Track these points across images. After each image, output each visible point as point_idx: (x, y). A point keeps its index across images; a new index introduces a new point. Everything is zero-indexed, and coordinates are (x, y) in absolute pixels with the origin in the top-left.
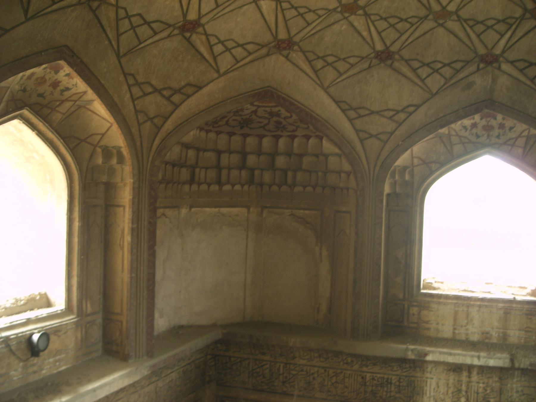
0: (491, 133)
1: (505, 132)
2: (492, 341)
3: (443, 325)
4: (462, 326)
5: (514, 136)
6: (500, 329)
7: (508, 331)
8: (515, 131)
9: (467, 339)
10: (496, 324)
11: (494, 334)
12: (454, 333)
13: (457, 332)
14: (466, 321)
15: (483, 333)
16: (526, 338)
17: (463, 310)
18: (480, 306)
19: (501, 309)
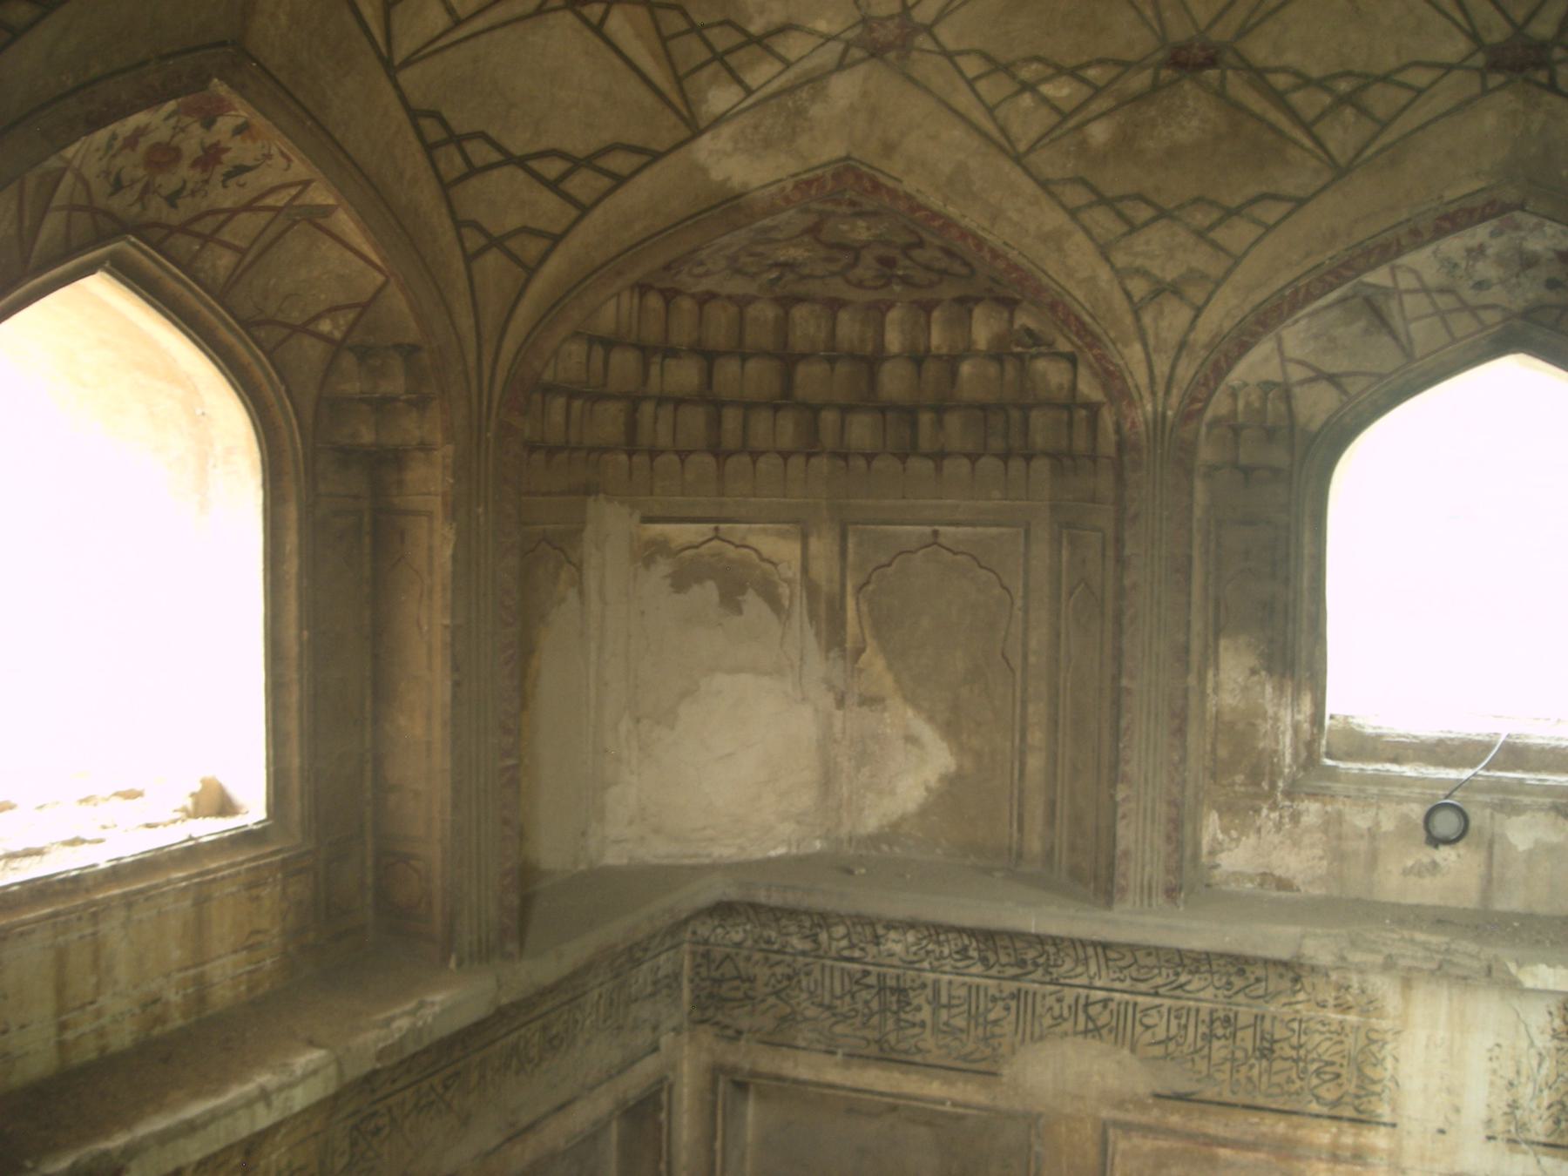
0: (159, 179)
1: (206, 182)
2: (170, 1027)
3: (23, 1027)
4: (82, 1007)
5: (228, 204)
6: (186, 969)
7: (207, 967)
8: (242, 186)
9: (103, 1049)
10: (176, 954)
11: (173, 997)
12: (62, 1046)
13: (69, 1035)
14: (93, 980)
15: (144, 1006)
16: (250, 972)
17: (81, 937)
18: (128, 901)
19: (185, 888)
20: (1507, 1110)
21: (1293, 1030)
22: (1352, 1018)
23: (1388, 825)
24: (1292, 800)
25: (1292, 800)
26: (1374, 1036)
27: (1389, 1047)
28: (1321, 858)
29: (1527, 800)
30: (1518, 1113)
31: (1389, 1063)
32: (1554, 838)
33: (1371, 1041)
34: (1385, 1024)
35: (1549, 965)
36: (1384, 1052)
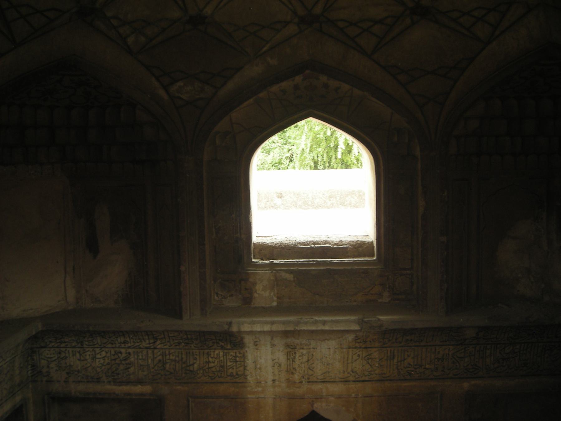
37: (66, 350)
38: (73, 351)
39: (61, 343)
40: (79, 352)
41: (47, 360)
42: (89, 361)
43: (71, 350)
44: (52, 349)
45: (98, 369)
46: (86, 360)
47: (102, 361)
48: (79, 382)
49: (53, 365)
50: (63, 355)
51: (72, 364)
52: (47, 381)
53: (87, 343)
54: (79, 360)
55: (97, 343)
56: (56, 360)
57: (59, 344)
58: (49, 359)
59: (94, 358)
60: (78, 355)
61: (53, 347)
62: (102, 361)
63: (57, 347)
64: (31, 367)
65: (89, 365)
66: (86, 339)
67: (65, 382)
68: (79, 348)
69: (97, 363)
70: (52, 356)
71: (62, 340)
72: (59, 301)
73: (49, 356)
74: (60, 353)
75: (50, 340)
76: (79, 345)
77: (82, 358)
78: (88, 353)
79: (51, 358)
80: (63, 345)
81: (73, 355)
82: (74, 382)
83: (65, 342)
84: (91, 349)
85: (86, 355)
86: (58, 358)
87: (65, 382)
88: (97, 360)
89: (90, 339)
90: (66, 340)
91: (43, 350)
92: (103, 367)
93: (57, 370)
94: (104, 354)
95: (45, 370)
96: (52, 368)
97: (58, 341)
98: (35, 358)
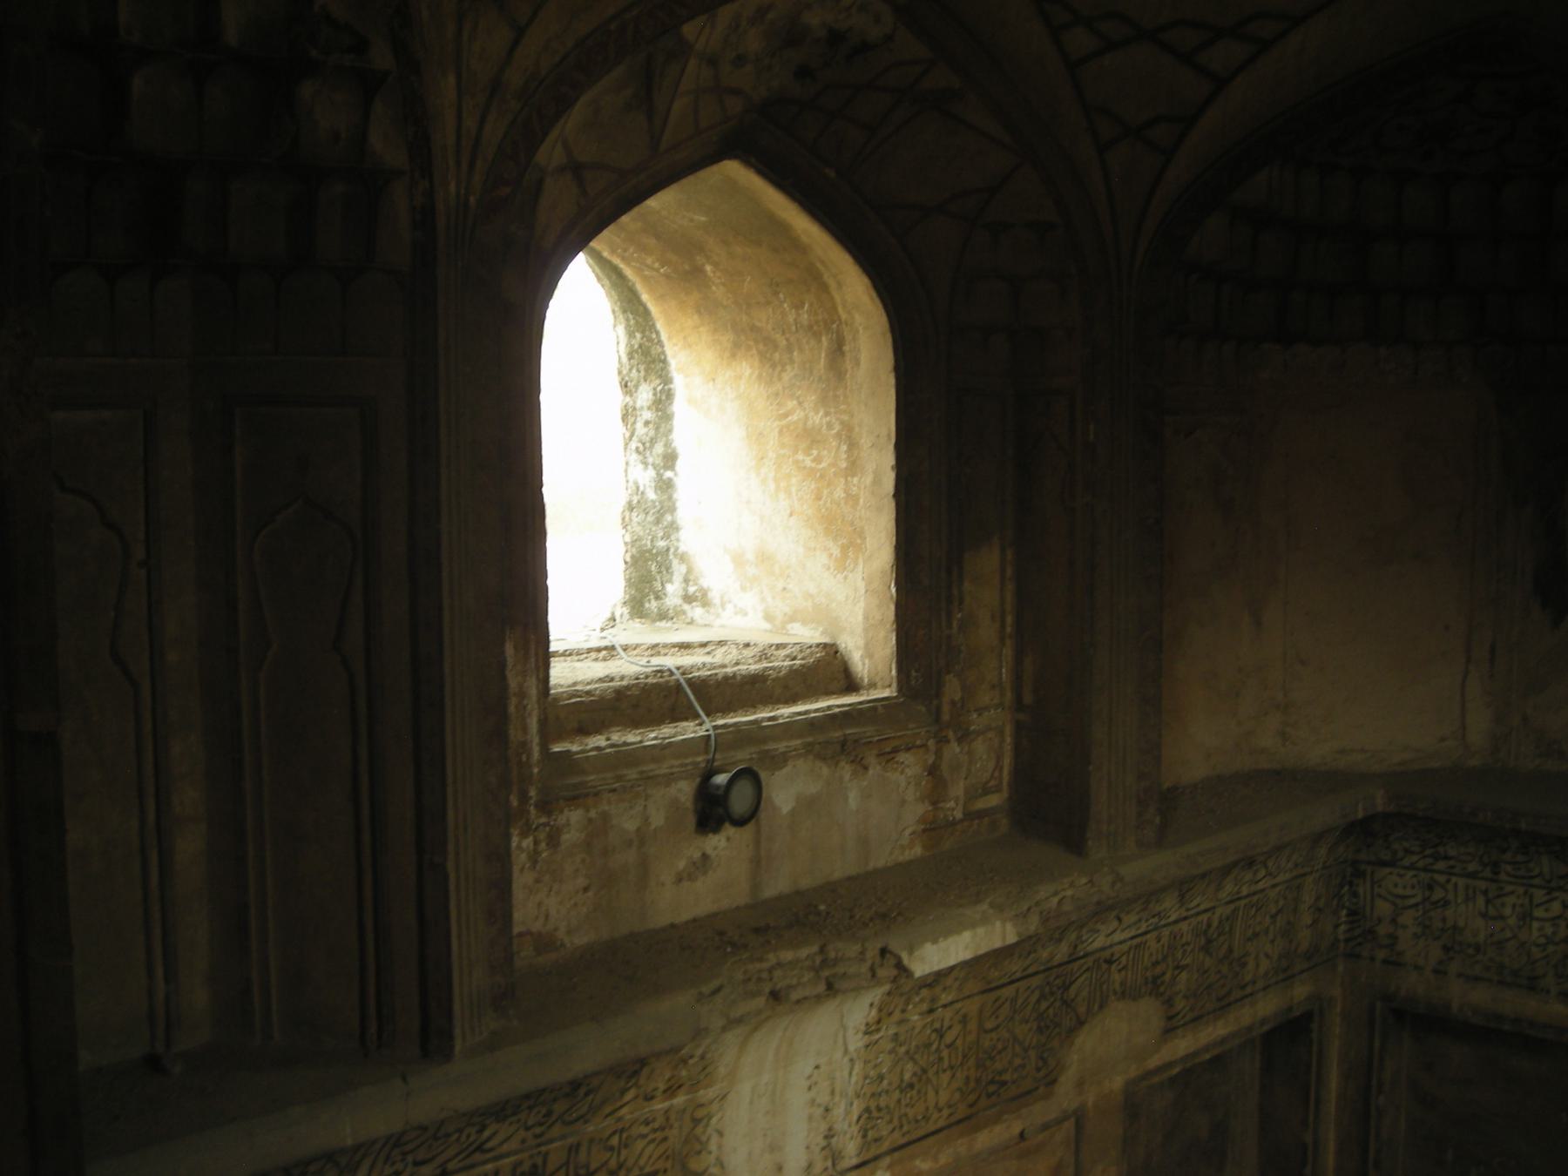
20: (824, 1143)
21: (612, 1149)
22: (680, 1100)
23: (657, 819)
24: (549, 814)
25: (549, 814)
26: (700, 1113)
27: (714, 1120)
28: (586, 889)
29: (781, 746)
30: (834, 1140)
31: (713, 1146)
32: (813, 788)
33: (696, 1121)
34: (711, 1093)
35: (935, 941)
36: (709, 1130)
37: (1448, 881)
38: (1467, 888)
39: (1436, 857)
40: (1485, 893)
41: (1394, 904)
42: (1512, 921)
43: (1461, 882)
44: (1411, 873)
45: (1534, 949)
46: (1502, 917)
47: (1549, 930)
48: (1477, 979)
49: (1407, 918)
50: (1438, 894)
51: (1461, 923)
52: (1385, 962)
53: (1509, 868)
54: (1484, 915)
55: (1540, 874)
56: (1416, 905)
57: (1430, 860)
58: (1398, 901)
59: (1526, 917)
60: (1481, 901)
61: (1412, 867)
62: (1549, 930)
63: (1425, 870)
64: (1348, 915)
65: (1508, 934)
66: (1508, 856)
67: (1436, 971)
68: (1483, 879)
69: (1535, 933)
70: (1409, 892)
71: (1441, 849)
72: (1443, 739)
73: (1400, 891)
74: (1430, 888)
75: (1406, 844)
76: (1487, 873)
77: (1492, 911)
78: (1510, 900)
79: (1404, 897)
80: (1441, 865)
81: (1467, 899)
82: (1460, 975)
83: (1446, 858)
84: (1521, 890)
85: (1503, 905)
86: (1425, 900)
87: (1436, 971)
88: (1535, 925)
89: (1520, 858)
90: (1452, 853)
91: (1388, 870)
92: (1551, 948)
93: (1416, 936)
94: (1556, 907)
95: (1382, 930)
96: (1405, 927)
97: (1428, 852)
98: (1361, 890)
